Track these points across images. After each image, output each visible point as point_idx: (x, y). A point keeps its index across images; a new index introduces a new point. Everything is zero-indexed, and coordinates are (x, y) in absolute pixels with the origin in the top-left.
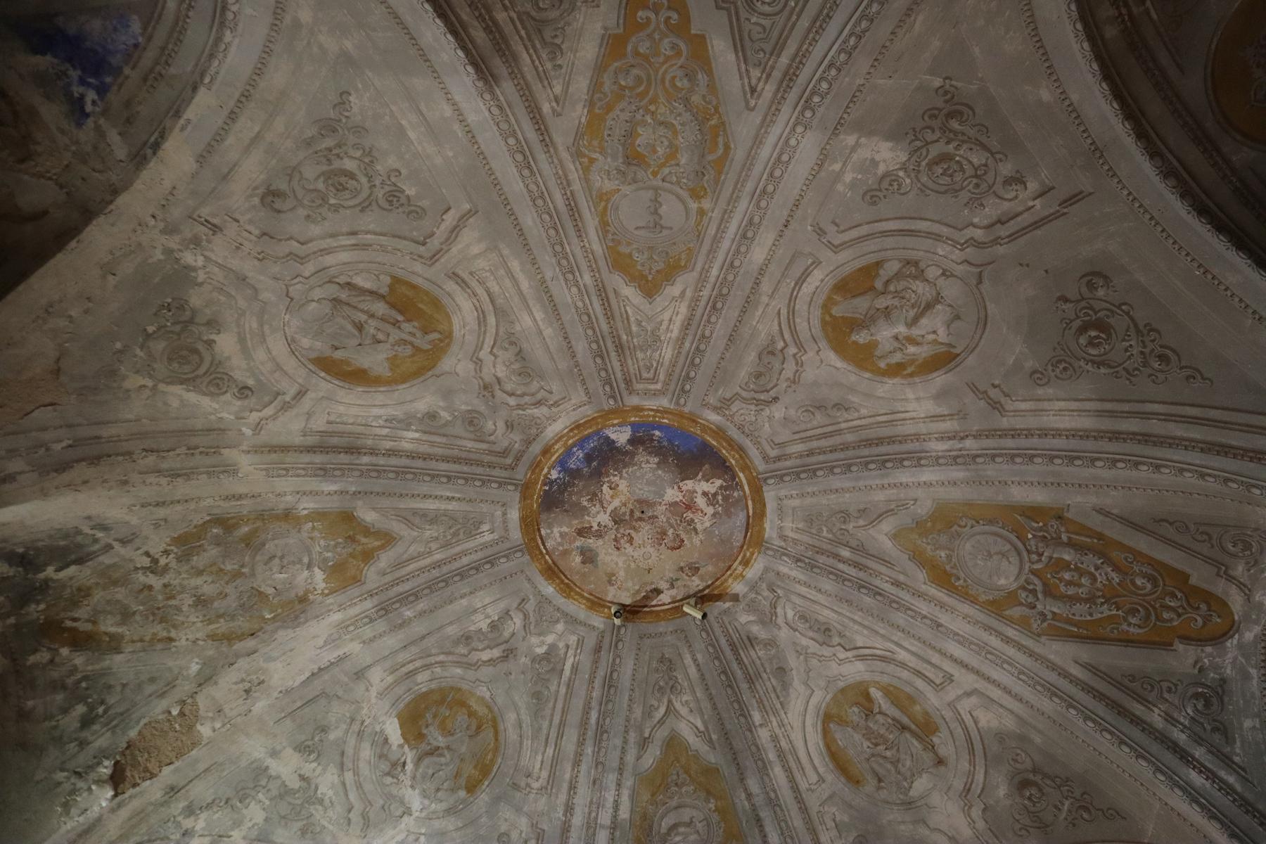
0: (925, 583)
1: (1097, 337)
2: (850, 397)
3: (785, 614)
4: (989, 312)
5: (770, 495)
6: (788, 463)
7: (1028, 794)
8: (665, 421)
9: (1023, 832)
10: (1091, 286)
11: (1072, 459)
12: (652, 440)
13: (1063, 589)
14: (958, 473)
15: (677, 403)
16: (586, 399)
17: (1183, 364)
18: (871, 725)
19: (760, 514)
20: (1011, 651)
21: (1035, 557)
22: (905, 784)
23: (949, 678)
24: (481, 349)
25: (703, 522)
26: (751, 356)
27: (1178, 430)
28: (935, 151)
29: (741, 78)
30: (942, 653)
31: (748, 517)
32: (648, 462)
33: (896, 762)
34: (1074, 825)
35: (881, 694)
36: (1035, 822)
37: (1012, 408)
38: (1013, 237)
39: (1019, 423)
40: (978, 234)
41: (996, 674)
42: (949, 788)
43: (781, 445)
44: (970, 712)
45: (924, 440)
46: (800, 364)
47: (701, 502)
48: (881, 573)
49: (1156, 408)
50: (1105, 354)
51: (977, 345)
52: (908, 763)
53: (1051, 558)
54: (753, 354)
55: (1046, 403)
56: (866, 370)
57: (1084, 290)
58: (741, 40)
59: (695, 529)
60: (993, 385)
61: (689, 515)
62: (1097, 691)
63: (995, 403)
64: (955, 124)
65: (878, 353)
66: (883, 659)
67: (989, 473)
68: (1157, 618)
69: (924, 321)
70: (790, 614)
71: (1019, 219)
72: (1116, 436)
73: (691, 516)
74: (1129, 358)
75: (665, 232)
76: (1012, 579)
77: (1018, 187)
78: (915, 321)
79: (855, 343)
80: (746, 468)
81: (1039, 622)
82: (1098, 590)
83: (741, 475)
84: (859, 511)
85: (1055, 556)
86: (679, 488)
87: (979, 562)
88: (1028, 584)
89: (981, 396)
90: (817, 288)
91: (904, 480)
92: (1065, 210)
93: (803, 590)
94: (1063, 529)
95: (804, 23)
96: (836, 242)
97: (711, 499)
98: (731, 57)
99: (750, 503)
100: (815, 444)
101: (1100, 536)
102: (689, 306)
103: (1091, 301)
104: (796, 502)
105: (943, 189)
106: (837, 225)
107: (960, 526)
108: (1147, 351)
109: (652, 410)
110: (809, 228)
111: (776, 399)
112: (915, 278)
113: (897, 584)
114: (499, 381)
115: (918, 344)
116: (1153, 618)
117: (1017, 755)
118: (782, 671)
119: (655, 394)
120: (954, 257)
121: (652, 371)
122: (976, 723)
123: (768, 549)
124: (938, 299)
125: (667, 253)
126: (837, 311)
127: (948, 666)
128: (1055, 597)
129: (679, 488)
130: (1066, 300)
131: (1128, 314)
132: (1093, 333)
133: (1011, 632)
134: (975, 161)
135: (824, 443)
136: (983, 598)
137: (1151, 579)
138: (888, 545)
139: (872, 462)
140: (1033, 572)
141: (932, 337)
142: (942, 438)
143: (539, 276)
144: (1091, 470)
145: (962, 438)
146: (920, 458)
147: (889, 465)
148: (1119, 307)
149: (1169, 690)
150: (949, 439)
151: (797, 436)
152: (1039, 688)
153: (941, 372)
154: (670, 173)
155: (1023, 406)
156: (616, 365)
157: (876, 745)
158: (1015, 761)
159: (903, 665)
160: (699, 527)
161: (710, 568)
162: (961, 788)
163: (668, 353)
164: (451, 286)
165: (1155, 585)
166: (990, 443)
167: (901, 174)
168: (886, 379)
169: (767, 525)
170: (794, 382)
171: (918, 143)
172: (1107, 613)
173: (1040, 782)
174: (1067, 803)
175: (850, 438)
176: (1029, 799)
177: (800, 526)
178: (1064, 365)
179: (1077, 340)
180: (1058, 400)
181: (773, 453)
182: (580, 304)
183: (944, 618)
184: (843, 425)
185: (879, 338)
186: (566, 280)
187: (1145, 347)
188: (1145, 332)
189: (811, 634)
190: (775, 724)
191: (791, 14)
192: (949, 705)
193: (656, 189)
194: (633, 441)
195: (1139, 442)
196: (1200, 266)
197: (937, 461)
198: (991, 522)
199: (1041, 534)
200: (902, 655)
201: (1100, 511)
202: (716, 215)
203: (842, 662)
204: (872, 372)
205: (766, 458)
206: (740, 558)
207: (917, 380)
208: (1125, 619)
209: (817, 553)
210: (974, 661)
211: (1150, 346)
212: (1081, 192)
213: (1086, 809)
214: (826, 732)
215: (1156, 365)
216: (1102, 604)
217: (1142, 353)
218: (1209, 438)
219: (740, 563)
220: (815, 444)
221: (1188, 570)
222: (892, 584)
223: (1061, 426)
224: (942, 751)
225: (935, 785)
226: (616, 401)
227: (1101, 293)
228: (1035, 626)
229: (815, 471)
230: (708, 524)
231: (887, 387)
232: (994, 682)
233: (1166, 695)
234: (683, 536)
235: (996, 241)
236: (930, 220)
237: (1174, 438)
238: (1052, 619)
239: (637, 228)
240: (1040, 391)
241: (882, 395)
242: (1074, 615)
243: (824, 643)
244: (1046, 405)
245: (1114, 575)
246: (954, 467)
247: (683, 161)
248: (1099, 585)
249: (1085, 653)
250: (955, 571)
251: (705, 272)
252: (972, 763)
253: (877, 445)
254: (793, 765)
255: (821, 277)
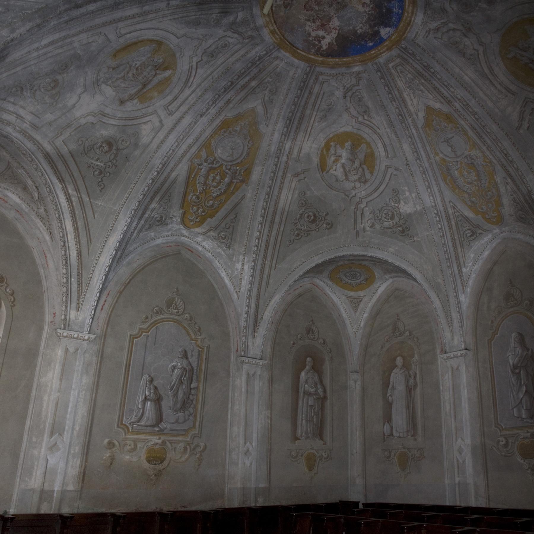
0: (225, 116)
1: (310, 218)
2: (326, 123)
3: (232, 38)
4: (333, 191)
5: (302, 65)
6: (312, 81)
7: (104, 146)
8: (373, 52)
9: (81, 142)
10: (329, 224)
11: (268, 194)
12: (369, 39)
13: (212, 175)
14: (273, 149)
15: (376, 64)
16: (416, 41)
17: (295, 241)
18: (150, 68)
19: (295, 54)
20: (184, 147)
21: (229, 167)
22: (110, 82)
23: (171, 114)
24: (483, 51)
25: (309, 27)
26: (370, 104)
27: (274, 233)
28: (397, 219)
29: (459, 209)
30: (186, 113)
31: (298, 49)
32: (361, 28)
33: (124, 78)
34: (89, 167)
35: (167, 76)
36: (87, 148)
37: (294, 180)
38: (355, 213)
39: (287, 180)
40: (363, 206)
41: (172, 138)
42: (106, 106)
43: (322, 84)
44: (150, 121)
45: (292, 141)
46: (353, 117)
47: (321, 33)
48: (236, 96)
49: (282, 228)
50: (304, 218)
51: (323, 180)
52: (123, 85)
53: (227, 174)
54: (370, 106)
55: (292, 193)
56: (334, 136)
57: (328, 221)
58: (466, 220)
59: (309, 20)
60: (305, 178)
61: (318, 23)
62: (164, 184)
63: (298, 175)
64: (400, 229)
65: (338, 146)
66: (187, 80)
67: (270, 161)
68: (193, 205)
69: (342, 170)
70: (231, 40)
71: (360, 219)
72: (275, 213)
73: (317, 24)
74: (301, 225)
75: (442, 140)
76: (220, 156)
77: (371, 225)
78: (343, 166)
79: (348, 141)
80: (322, 63)
81: (198, 163)
82: (210, 188)
83: (321, 59)
84: (273, 100)
85: (228, 175)
86: (336, 29)
87: (230, 144)
88: (217, 162)
89: (302, 171)
90: (378, 148)
91: (279, 125)
92: (355, 231)
93: (242, 52)
94: (238, 181)
95: (456, 238)
96: (389, 170)
97: (319, 39)
98: (466, 214)
99: (304, 54)
100: (313, 97)
101: (233, 193)
102: (410, 111)
103: (323, 222)
104: (291, 73)
105: (383, 209)
106: (395, 175)
107: (249, 141)
108: (302, 231)
109: (383, 53)
110: (401, 168)
111: (345, 97)
112: (359, 179)
113: (229, 102)
114: (466, 36)
115: (334, 162)
116: (194, 204)
117: (126, 142)
118: (197, 23)
119: (388, 61)
120: (359, 194)
121: (399, 71)
122: (144, 123)
123: (274, 47)
124: (347, 179)
125: (436, 131)
126: (364, 146)
127: (177, 115)
128: (209, 171)
129: (336, 29)
130: (326, 215)
131: (315, 230)
132: (312, 218)
133: (194, 149)
134: (386, 223)
135: (312, 100)
136: (213, 141)
137: (212, 206)
138: (251, 105)
139: (292, 116)
140: (222, 165)
141: (334, 168)
142: (291, 149)
143: (477, 100)
144: (262, 200)
145: (288, 156)
146: (285, 136)
147: (288, 122)
148: (318, 228)
149: (164, 208)
150: (289, 151)
151: (322, 93)
152: (166, 158)
153: (319, 163)
154: (457, 165)
155: (293, 185)
156: (416, 66)
157: (137, 69)
158: (123, 141)
159: (182, 91)
160: (309, 23)
161: (282, 14)
162: (105, 112)
163: (400, 84)
164: (513, 87)
165: (208, 207)
166: (282, 167)
167: (397, 205)
168: (325, 141)
169: (287, 54)
170: (347, 109)
171: (402, 217)
172: (198, 189)
173: (112, 152)
174: (102, 164)
175: (308, 112)
176: (101, 146)
177: (278, 69)
178: (304, 204)
179: (312, 212)
180: (292, 197)
181: (321, 78)
182: (452, 90)
183: (205, 120)
184: (315, 113)
185: (344, 151)
186: (465, 101)
187: (303, 231)
188: (308, 233)
189: (213, 47)
190: (167, 12)
191: (461, 236)
192: (155, 111)
193: (457, 157)
194: (377, 33)
195: (271, 221)
196: (323, 253)
197: (282, 142)
198: (248, 154)
199: (238, 172)
200: (187, 92)
201: (243, 197)
202: (432, 156)
203: (191, 58)
204: (331, 138)
205: (321, 73)
206: (277, 31)
207: (320, 152)
208: (194, 195)
209: (260, 70)
210: (180, 128)
211: (303, 233)
212: (358, 237)
213: (100, 173)
214: (151, 41)
215: (296, 232)
216: (203, 188)
217: (301, 229)
218: (270, 243)
219: (275, 30)
220: (313, 97)
221: (214, 218)
222: (229, 100)
223: (282, 195)
224: (129, 104)
225: (107, 98)
226: (402, 47)
227: (325, 225)
228: (196, 160)
229: (301, 90)
230: (307, 28)
231: (322, 139)
232: (167, 137)
233: (162, 207)
234: (309, 13)
235: (357, 208)
236: (375, 198)
237: (271, 232)
238: (198, 168)
239: (453, 137)
240: (297, 192)
241: (320, 136)
242: (200, 177)
243: (205, 52)
244: (291, 192)
245: (215, 194)
246: (277, 148)
247: (456, 172)
248: (212, 188)
249: (182, 179)
250: (228, 132)
251: (417, 130)
252: (120, 119)
253: (299, 121)
254: (137, 19)
255: (381, 153)
